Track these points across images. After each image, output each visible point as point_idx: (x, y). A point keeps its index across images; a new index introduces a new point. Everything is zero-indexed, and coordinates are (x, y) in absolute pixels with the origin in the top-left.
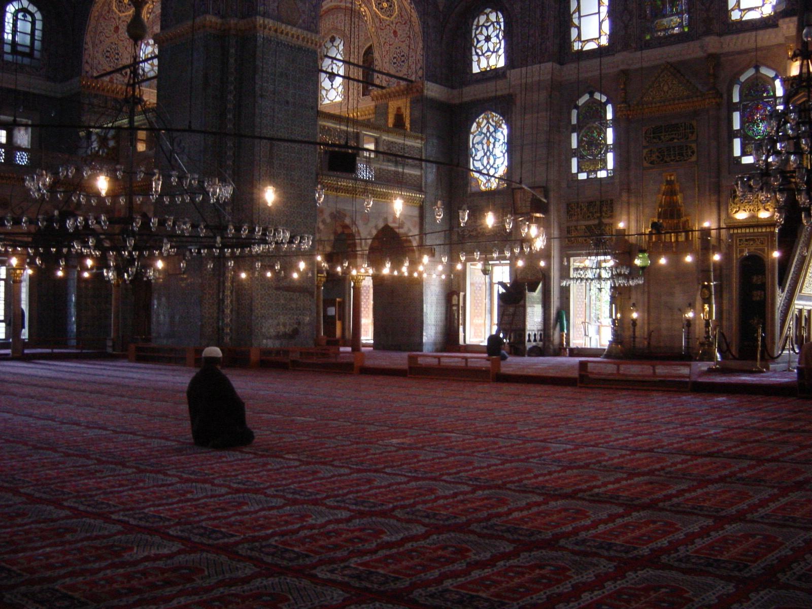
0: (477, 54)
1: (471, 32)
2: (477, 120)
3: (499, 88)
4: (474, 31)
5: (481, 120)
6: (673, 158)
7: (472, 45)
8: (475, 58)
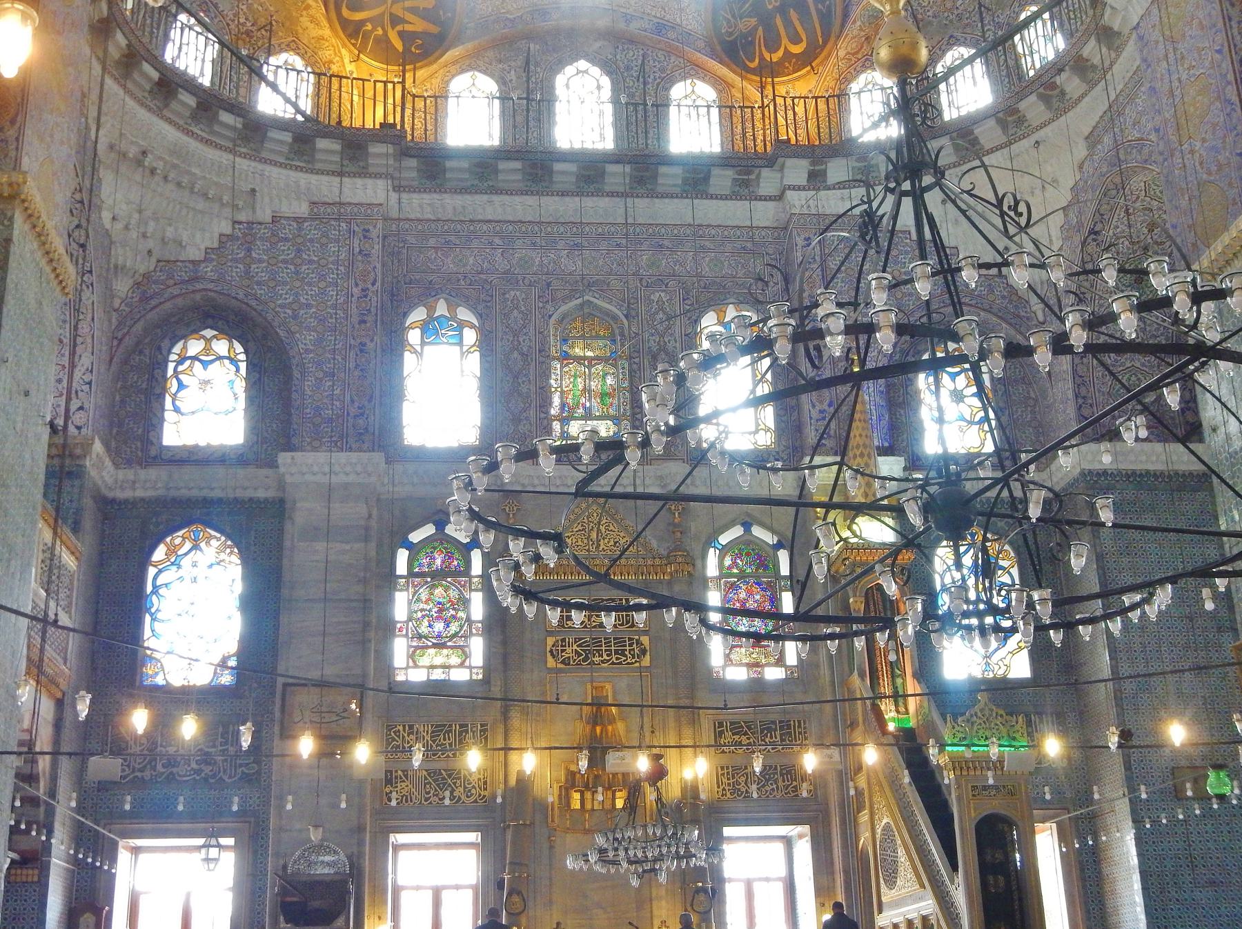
0: (177, 410)
1: (166, 367)
2: (168, 540)
3: (221, 484)
4: (171, 366)
5: (178, 541)
6: (605, 657)
7: (164, 390)
8: (169, 416)
